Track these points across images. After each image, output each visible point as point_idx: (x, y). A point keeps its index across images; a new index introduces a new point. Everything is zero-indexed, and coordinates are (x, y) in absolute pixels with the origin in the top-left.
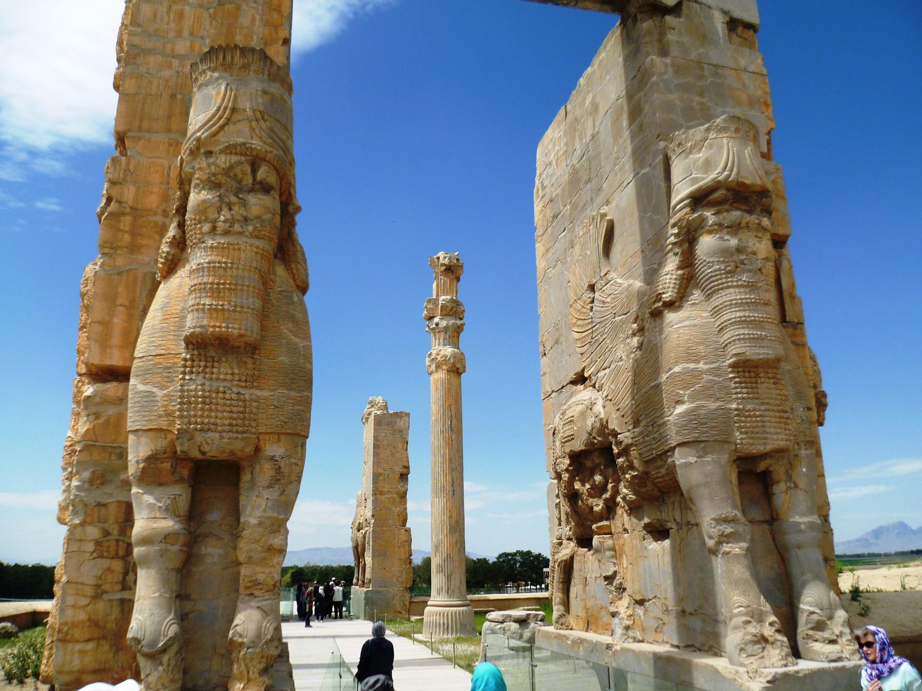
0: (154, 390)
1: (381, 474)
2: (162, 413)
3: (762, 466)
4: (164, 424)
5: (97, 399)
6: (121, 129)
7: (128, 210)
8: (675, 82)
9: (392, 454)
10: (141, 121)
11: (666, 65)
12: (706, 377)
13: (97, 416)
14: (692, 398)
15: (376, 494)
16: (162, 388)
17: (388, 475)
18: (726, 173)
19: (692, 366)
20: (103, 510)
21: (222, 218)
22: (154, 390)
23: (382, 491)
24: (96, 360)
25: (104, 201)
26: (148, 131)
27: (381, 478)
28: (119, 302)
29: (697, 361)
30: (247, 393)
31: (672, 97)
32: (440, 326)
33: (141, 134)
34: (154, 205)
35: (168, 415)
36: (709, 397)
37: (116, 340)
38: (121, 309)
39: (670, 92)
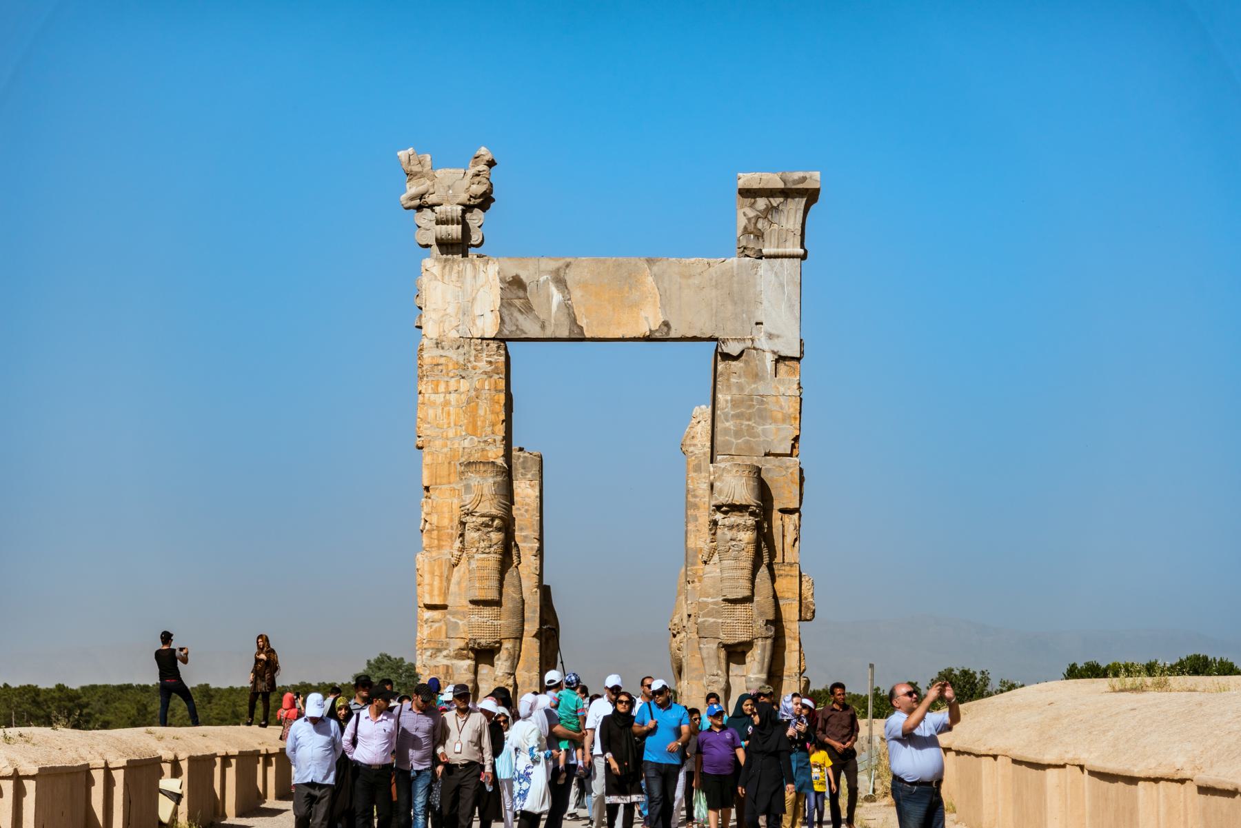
0: (459, 621)
2: (462, 631)
3: (739, 649)
4: (463, 636)
5: (430, 620)
6: (426, 484)
7: (435, 528)
8: (732, 413)
10: (436, 479)
11: (727, 401)
12: (711, 606)
13: (431, 627)
14: (703, 617)
15: (693, 582)
16: (461, 620)
18: (727, 499)
19: (705, 599)
20: (437, 669)
21: (481, 547)
22: (459, 621)
24: (428, 602)
25: (423, 522)
26: (440, 484)
28: (436, 574)
29: (708, 597)
30: (496, 623)
31: (727, 424)
33: (437, 486)
34: (447, 524)
35: (465, 632)
36: (710, 616)
37: (436, 592)
38: (437, 578)
39: (727, 421)
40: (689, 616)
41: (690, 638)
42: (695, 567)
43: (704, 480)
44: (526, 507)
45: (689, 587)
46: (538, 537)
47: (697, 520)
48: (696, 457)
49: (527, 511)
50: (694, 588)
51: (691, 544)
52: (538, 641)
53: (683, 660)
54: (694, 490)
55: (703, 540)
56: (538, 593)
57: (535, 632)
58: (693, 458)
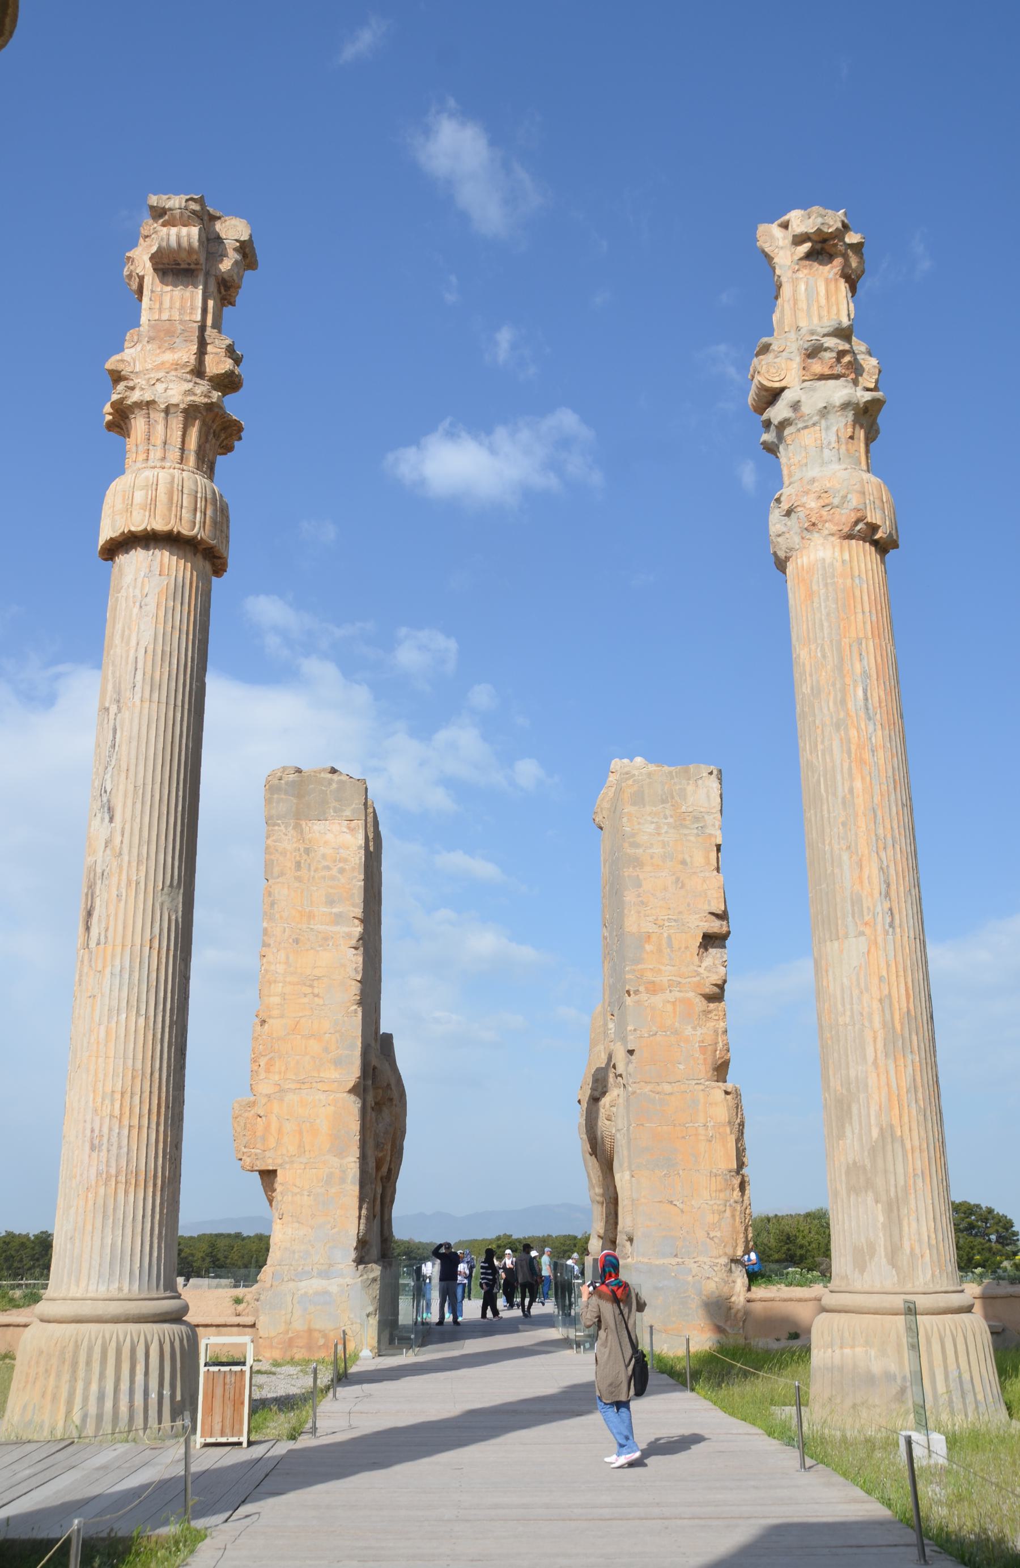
1: (648, 937)
9: (678, 880)
15: (637, 992)
17: (669, 937)
23: (653, 982)
27: (648, 947)
32: (805, 409)
40: (631, 1052)
41: (634, 1093)
42: (639, 967)
43: (649, 818)
44: (341, 865)
45: (629, 1001)
46: (360, 915)
47: (640, 886)
48: (634, 781)
49: (342, 871)
50: (638, 1003)
51: (632, 923)
52: (358, 1100)
53: (618, 1136)
54: (633, 835)
55: (651, 919)
56: (360, 1014)
57: (351, 1084)
58: (630, 782)
